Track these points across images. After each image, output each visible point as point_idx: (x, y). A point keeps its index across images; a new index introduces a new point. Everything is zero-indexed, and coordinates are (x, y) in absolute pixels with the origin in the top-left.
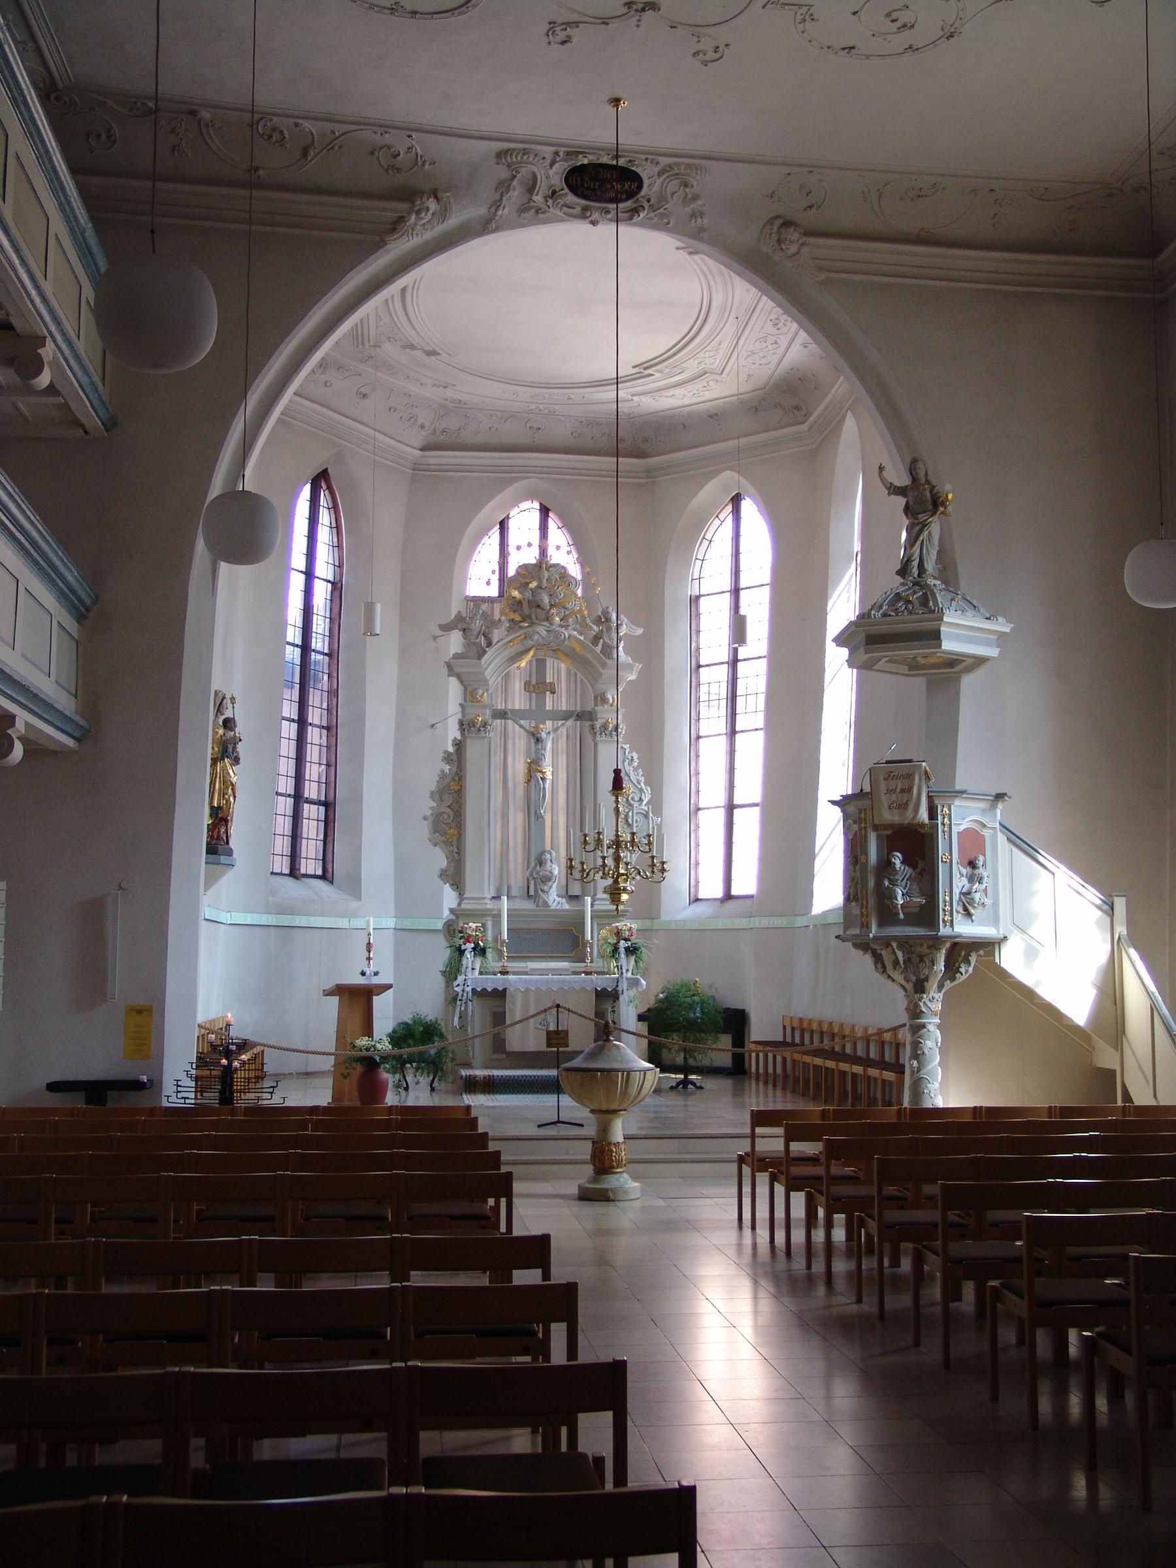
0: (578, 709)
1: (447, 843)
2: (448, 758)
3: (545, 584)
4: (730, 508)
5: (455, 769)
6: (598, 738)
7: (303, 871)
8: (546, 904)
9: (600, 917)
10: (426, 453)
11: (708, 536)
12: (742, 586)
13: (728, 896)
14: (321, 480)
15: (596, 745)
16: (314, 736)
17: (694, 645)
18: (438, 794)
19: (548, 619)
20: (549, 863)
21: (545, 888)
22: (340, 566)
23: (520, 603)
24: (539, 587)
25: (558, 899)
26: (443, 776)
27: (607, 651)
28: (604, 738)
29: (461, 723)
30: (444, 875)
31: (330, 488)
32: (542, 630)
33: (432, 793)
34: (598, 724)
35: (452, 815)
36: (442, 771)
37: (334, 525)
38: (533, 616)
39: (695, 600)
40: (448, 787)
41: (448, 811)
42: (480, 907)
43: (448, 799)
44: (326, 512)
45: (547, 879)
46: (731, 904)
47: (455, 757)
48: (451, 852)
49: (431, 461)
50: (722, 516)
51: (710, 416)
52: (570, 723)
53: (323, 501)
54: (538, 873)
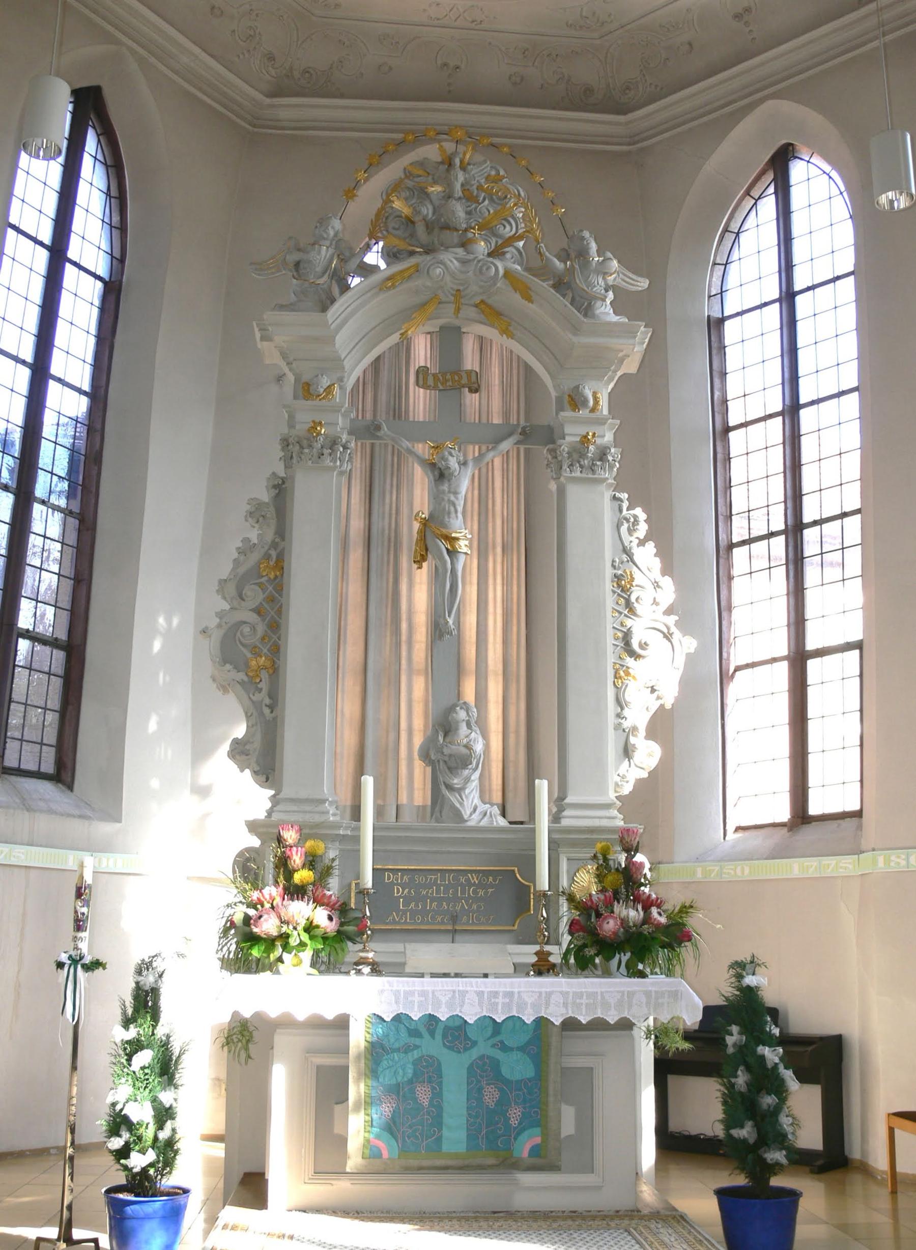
0: (522, 422)
1: (250, 685)
2: (256, 513)
3: (458, 191)
4: (770, 176)
5: (270, 535)
6: (566, 472)
8: (458, 816)
9: (574, 844)
11: (734, 227)
12: (797, 287)
13: (801, 817)
14: (89, 105)
15: (561, 492)
16: (47, 524)
17: (717, 394)
18: (236, 586)
19: (464, 244)
20: (463, 730)
21: (456, 782)
22: (122, 261)
23: (410, 222)
24: (448, 196)
25: (482, 807)
26: (246, 549)
28: (577, 474)
29: (285, 443)
30: (239, 751)
31: (109, 137)
32: (451, 259)
33: (222, 583)
35: (261, 629)
36: (246, 540)
37: (114, 192)
38: (436, 242)
39: (716, 325)
40: (255, 573)
41: (253, 617)
42: (317, 818)
43: (255, 595)
44: (100, 170)
45: (461, 762)
46: (809, 833)
47: (271, 512)
48: (257, 705)
49: (283, 114)
50: (756, 193)
51: (737, 17)
52: (506, 445)
53: (91, 143)
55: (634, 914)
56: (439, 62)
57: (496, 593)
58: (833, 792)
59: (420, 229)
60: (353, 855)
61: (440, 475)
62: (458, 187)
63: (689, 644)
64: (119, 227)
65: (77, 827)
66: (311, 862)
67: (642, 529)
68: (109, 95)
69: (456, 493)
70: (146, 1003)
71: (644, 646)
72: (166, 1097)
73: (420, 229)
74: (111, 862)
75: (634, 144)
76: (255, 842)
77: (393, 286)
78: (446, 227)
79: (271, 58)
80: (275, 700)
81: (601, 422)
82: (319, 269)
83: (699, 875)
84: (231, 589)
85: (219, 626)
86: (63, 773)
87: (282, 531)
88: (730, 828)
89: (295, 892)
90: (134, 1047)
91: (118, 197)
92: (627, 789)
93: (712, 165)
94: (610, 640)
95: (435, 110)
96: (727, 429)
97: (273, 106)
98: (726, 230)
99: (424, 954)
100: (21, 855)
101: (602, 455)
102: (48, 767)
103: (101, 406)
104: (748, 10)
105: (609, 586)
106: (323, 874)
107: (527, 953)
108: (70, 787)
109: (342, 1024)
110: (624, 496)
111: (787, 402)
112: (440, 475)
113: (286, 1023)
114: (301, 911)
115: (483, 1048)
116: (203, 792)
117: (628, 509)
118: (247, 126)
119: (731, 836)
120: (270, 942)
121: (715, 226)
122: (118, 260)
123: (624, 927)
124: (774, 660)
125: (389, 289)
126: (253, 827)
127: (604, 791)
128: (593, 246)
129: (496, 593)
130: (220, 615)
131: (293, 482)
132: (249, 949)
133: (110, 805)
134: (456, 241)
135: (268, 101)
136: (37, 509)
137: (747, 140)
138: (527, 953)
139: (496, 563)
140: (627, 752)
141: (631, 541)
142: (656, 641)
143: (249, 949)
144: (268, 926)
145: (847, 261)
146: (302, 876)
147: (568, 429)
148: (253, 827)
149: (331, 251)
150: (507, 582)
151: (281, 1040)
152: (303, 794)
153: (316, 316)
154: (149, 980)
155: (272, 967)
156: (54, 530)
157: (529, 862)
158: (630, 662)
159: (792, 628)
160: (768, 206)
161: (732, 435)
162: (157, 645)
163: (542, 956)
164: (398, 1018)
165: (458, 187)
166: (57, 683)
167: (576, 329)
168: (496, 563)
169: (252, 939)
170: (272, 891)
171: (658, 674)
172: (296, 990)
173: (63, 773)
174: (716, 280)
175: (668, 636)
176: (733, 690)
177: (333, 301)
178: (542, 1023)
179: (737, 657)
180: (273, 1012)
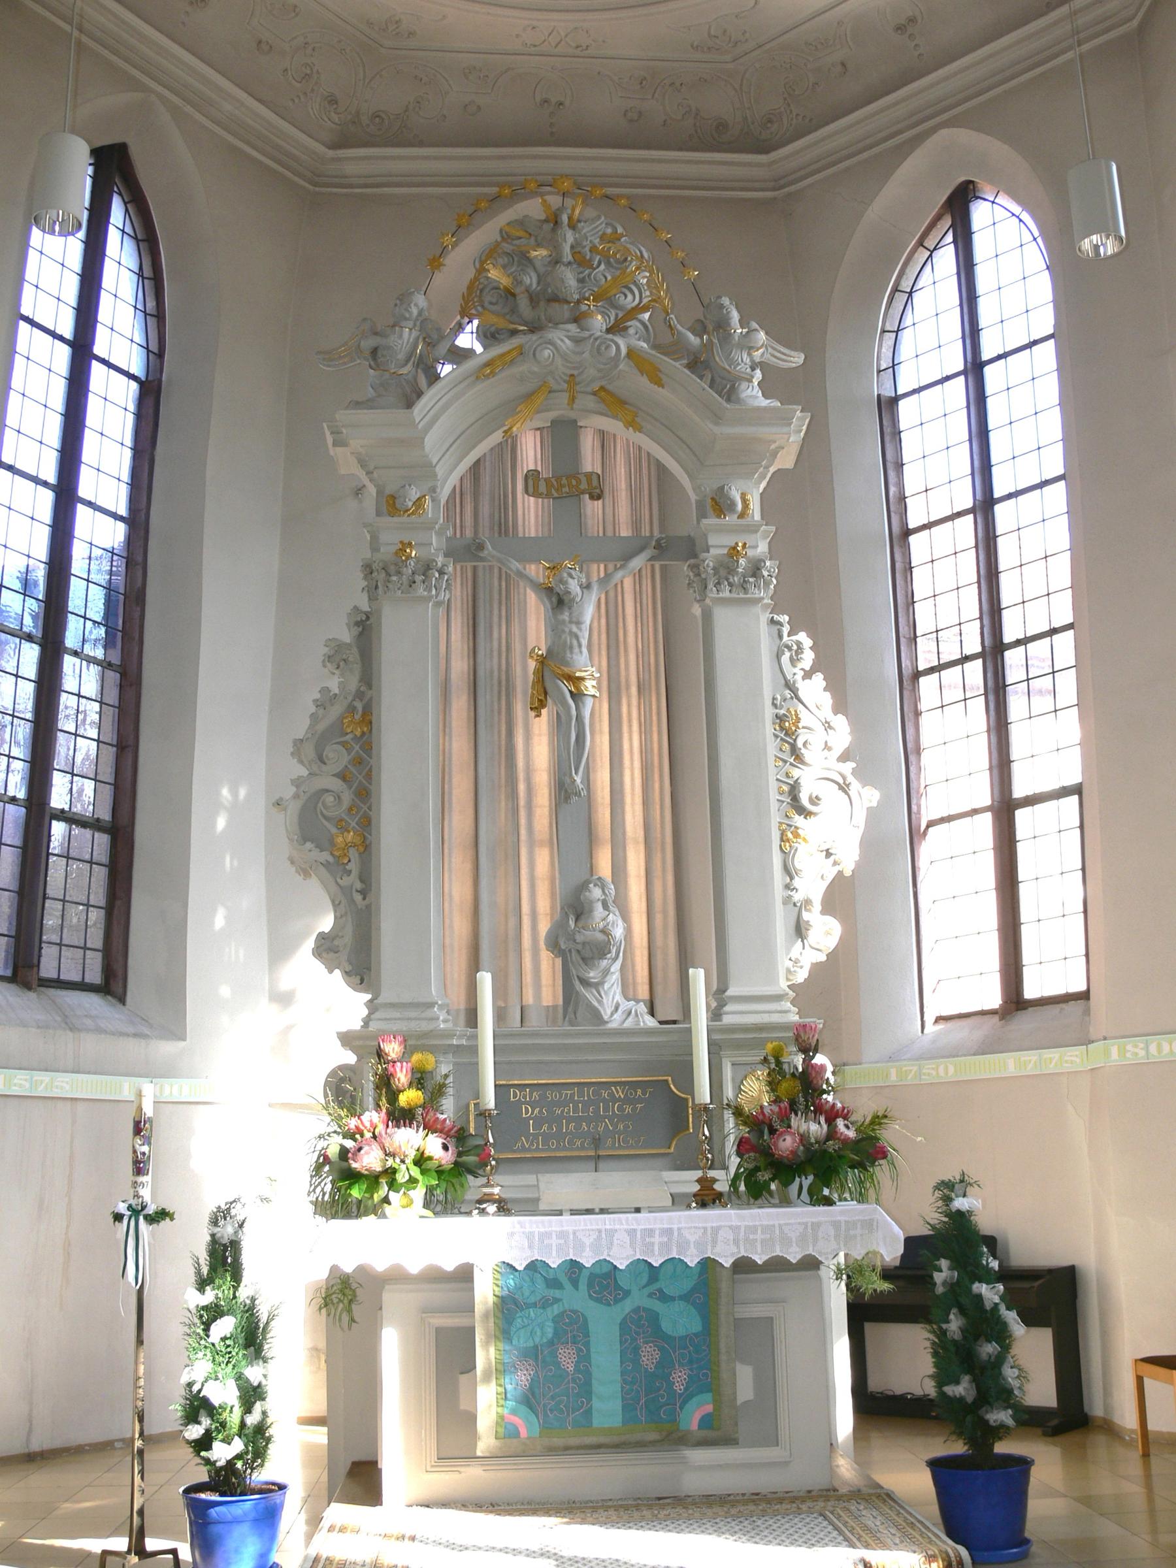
0: (656, 534)
1: (337, 867)
2: (336, 657)
4: (947, 221)
5: (353, 683)
6: (712, 593)
7: (48, 969)
8: (596, 1017)
9: (739, 1045)
10: (341, 153)
11: (906, 285)
12: (985, 357)
13: (1015, 1001)
14: (113, 167)
15: (707, 616)
16: (81, 680)
17: (893, 490)
18: (314, 747)
19: (578, 319)
20: (599, 908)
21: (593, 975)
22: (160, 355)
23: (510, 294)
24: (556, 261)
25: (625, 1005)
26: (325, 701)
27: (728, 387)
28: (726, 594)
29: (368, 569)
30: (326, 948)
32: (561, 337)
33: (298, 743)
34: (709, 560)
35: (347, 797)
36: (325, 690)
37: (147, 272)
39: (888, 406)
40: (337, 729)
41: (336, 784)
42: (425, 1026)
43: (338, 757)
45: (599, 950)
46: (1025, 1022)
47: (354, 655)
48: (346, 891)
49: (350, 169)
50: (930, 243)
51: (900, 29)
52: (637, 562)
53: (117, 213)
54: (571, 938)
55: (816, 1129)
56: (538, 99)
57: (632, 743)
58: (1052, 970)
59: (523, 303)
60: (470, 1069)
61: (559, 601)
62: (567, 249)
63: (870, 796)
64: (155, 313)
65: (132, 1049)
66: (420, 1079)
67: (808, 658)
68: (137, 154)
69: (579, 623)
70: (224, 1260)
71: (815, 800)
72: (254, 1373)
73: (523, 303)
74: (174, 1089)
75: (779, 189)
76: (350, 1058)
77: (493, 374)
78: (555, 299)
79: (332, 101)
80: (367, 883)
81: (753, 529)
82: (401, 356)
83: (893, 1077)
84: (309, 751)
85: (296, 796)
86: (112, 983)
87: (368, 677)
88: (929, 1018)
89: (401, 1117)
90: (213, 1313)
91: (152, 277)
92: (801, 976)
93: (876, 210)
94: (774, 796)
95: (535, 157)
96: (907, 533)
97: (339, 159)
98: (896, 290)
99: (562, 1186)
100: (65, 1084)
101: (756, 569)
102: (94, 975)
103: (142, 533)
104: (912, 20)
105: (769, 729)
106: (435, 1094)
107: (687, 1181)
108: (122, 1000)
109: (465, 1275)
110: (785, 618)
111: (979, 497)
112: (559, 601)
113: (397, 1277)
114: (408, 1139)
115: (638, 1299)
116: (284, 999)
117: (789, 635)
118: (307, 185)
119: (930, 1028)
120: (373, 1180)
121: (882, 284)
122: (156, 354)
123: (804, 1145)
124: (975, 812)
125: (487, 377)
126: (347, 1039)
127: (774, 980)
128: (735, 316)
129: (632, 743)
130: (297, 782)
131: (379, 618)
132: (348, 1187)
133: (172, 1023)
134: (567, 315)
135: (331, 153)
136: (69, 662)
137: (917, 179)
138: (687, 1181)
139: (630, 707)
140: (800, 930)
141: (795, 673)
142: (830, 793)
143: (348, 1187)
144: (370, 1160)
145: (1045, 322)
146: (409, 1097)
147: (713, 540)
148: (347, 1039)
149: (415, 333)
150: (645, 730)
151: (391, 1299)
152: (407, 998)
153: (401, 414)
154: (227, 1231)
155: (376, 1210)
156: (91, 687)
157: (685, 1070)
158: (799, 820)
159: (995, 771)
160: (946, 258)
161: (912, 539)
162: (221, 823)
163: (706, 1184)
164: (532, 1266)
165: (567, 249)
166: (101, 874)
167: (717, 418)
168: (630, 707)
169: (350, 1176)
170: (373, 1117)
171: (834, 833)
172: (406, 1237)
173: (112, 983)
174: (886, 351)
175: (844, 788)
176: (926, 850)
177: (420, 394)
178: (708, 1265)
179: (929, 809)
180: (380, 1265)
